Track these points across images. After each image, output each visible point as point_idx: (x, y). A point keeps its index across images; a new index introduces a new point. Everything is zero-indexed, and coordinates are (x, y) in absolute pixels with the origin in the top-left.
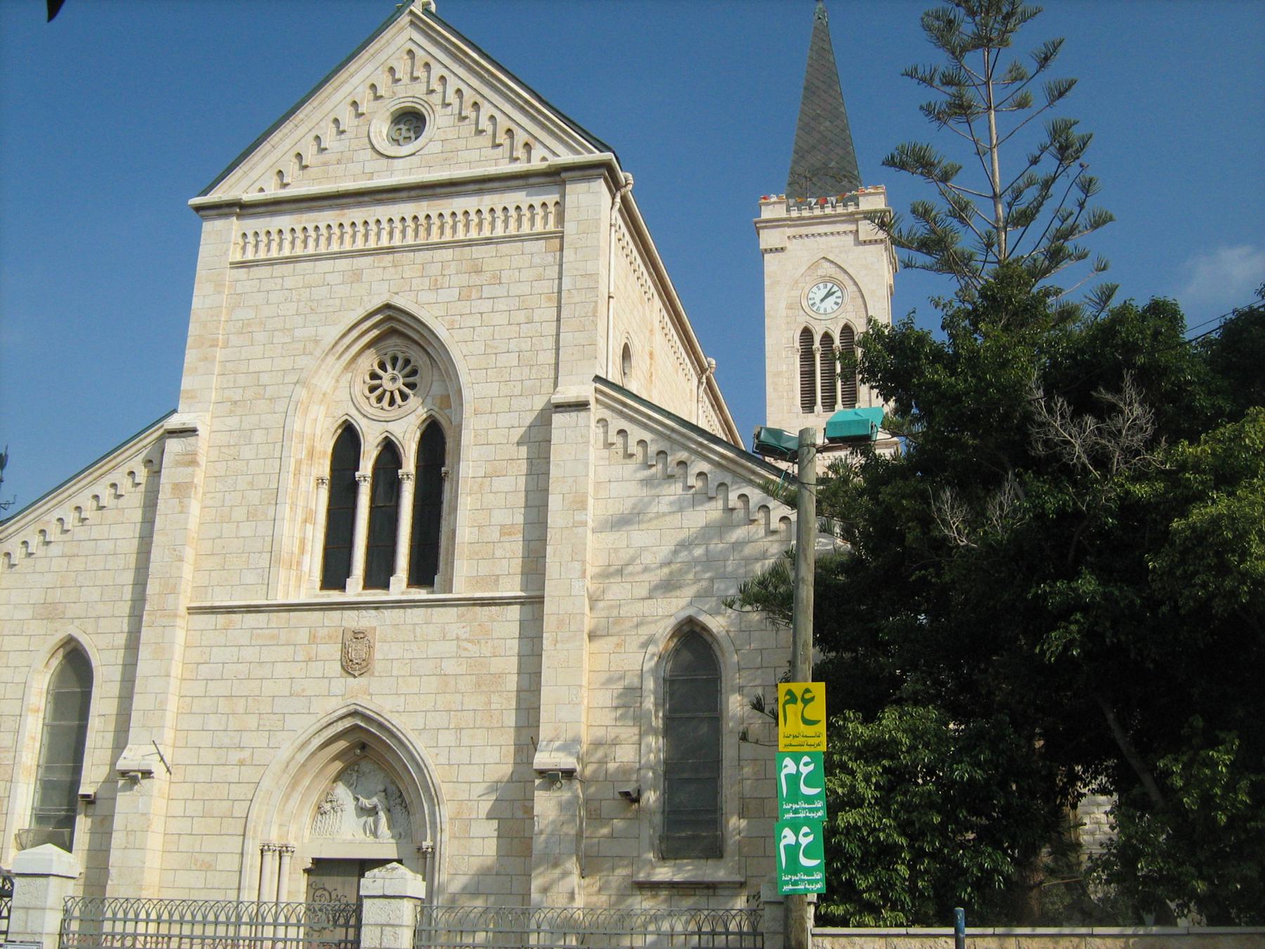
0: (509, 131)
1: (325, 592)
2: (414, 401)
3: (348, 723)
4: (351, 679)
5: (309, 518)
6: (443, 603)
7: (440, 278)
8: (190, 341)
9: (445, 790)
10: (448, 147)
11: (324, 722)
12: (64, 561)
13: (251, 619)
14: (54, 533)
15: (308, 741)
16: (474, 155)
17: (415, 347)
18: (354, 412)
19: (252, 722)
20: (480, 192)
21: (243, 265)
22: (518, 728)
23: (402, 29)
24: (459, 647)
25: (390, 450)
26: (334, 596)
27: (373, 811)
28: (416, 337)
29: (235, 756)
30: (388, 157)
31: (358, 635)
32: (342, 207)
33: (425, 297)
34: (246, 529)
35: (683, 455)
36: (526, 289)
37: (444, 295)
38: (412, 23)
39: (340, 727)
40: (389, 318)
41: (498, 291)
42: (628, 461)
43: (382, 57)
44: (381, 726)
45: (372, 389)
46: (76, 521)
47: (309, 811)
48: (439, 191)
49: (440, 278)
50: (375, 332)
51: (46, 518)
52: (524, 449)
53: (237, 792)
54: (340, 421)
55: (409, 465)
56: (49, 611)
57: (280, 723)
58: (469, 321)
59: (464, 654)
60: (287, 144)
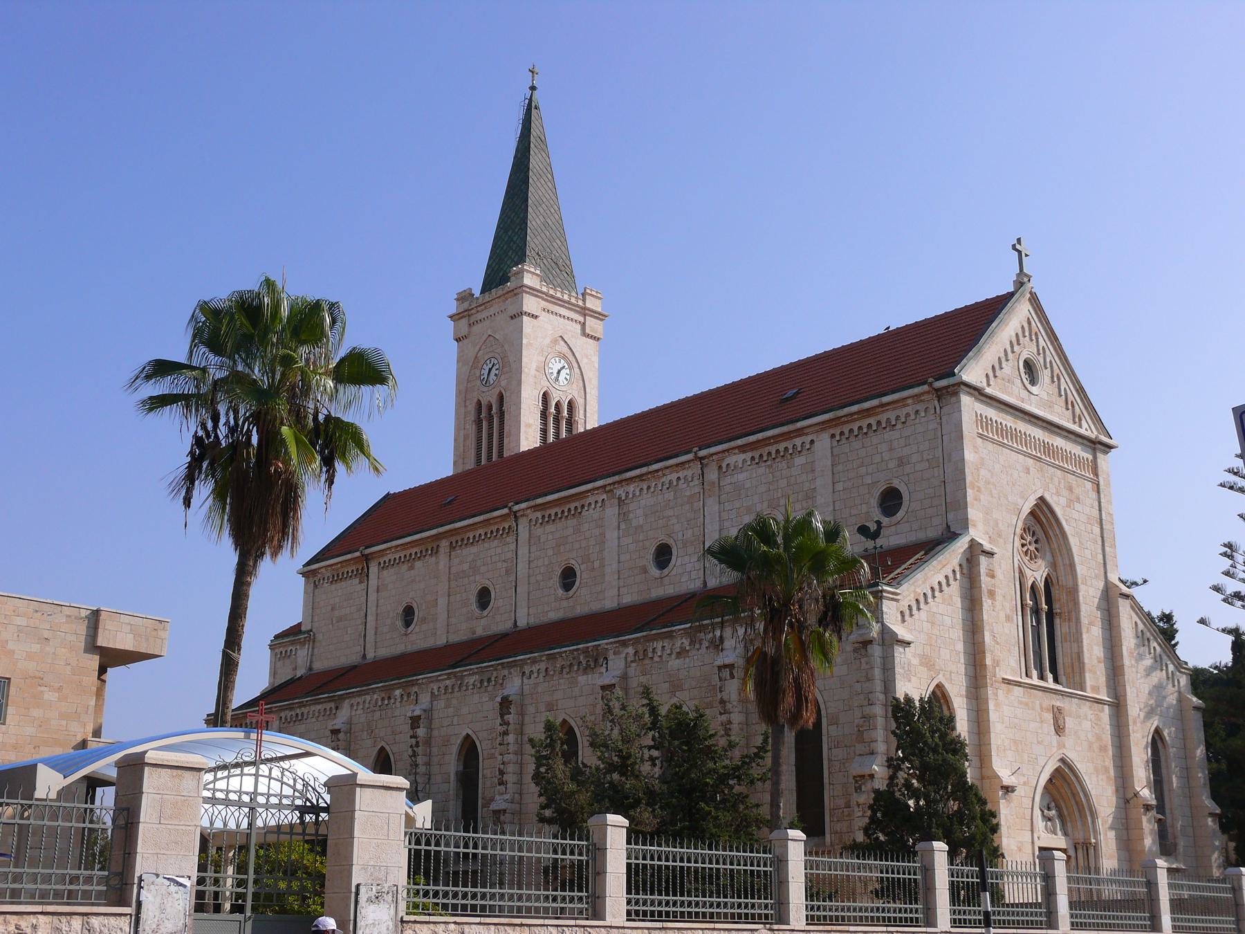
2: (1040, 561)
31: (1059, 709)
32: (1016, 417)
33: (1055, 498)
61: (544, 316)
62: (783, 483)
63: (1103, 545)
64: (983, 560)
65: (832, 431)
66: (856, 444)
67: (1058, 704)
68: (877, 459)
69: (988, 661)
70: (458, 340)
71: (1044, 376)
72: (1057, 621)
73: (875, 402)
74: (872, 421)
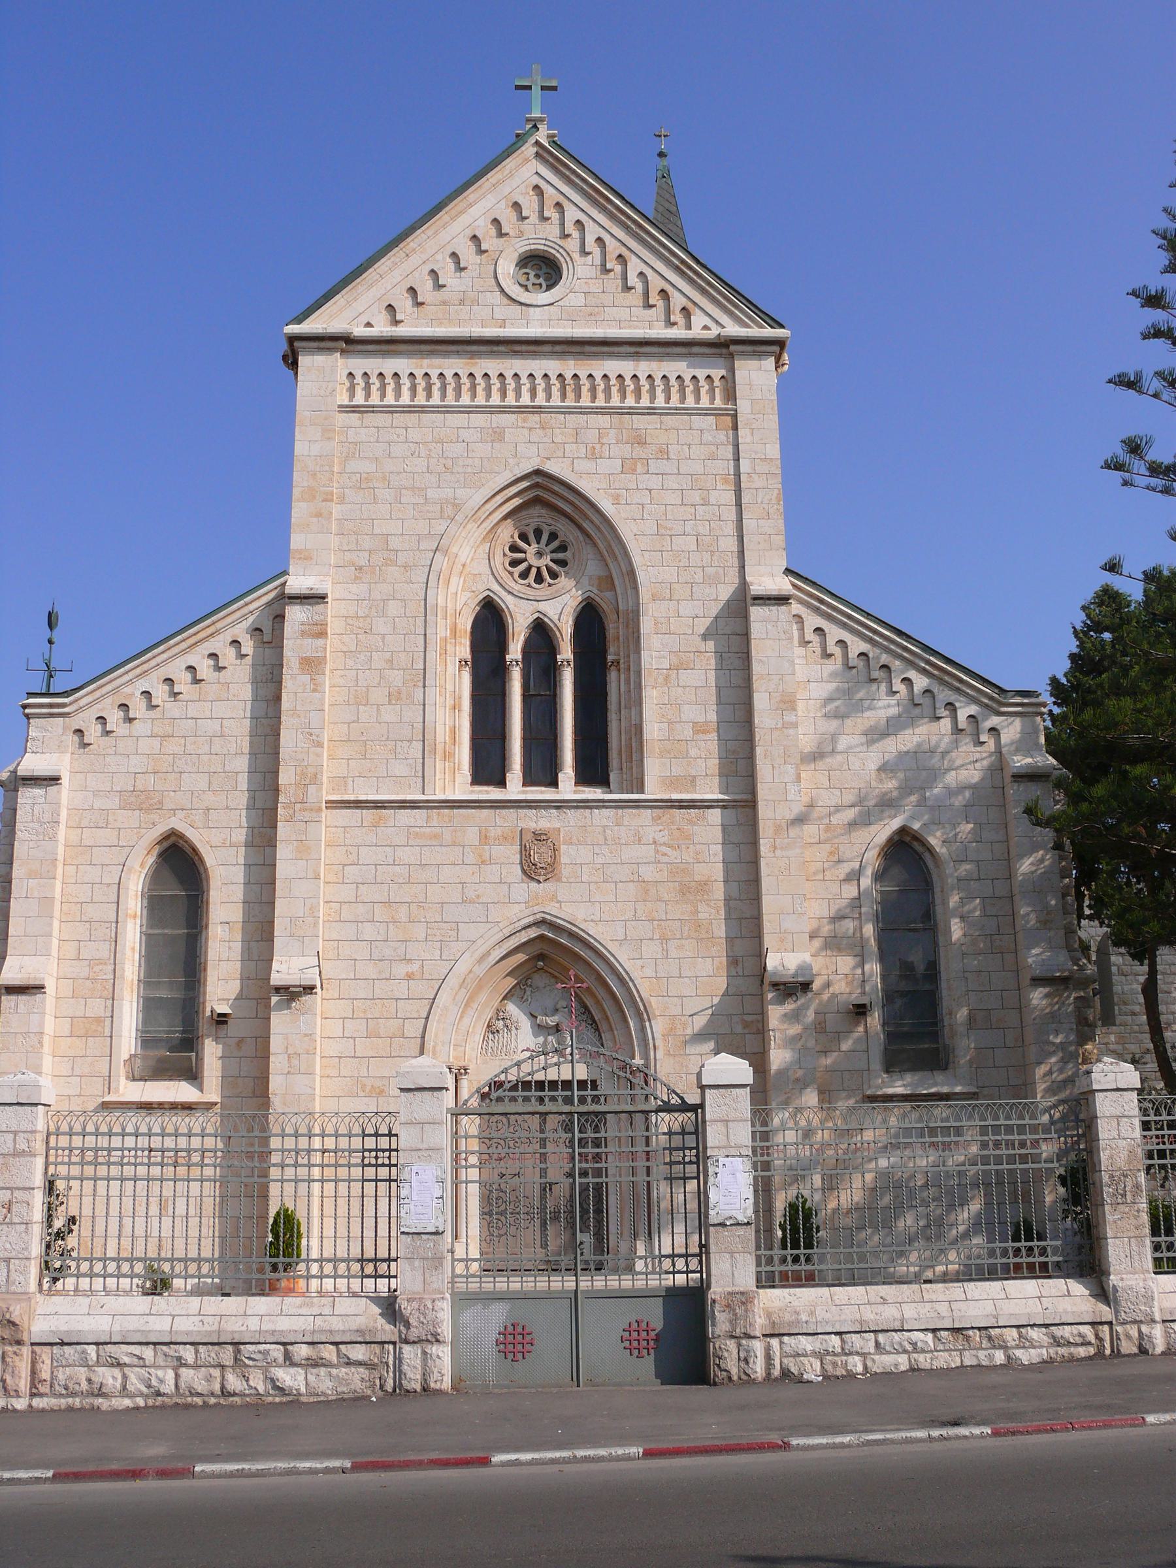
0: (663, 291)
1: (477, 788)
2: (564, 582)
3: (533, 933)
4: (533, 885)
5: (456, 707)
6: (636, 805)
7: (598, 447)
8: (296, 492)
9: (655, 1004)
10: (592, 300)
11: (507, 932)
12: (156, 742)
13: (405, 816)
14: (138, 707)
15: (488, 953)
16: (624, 313)
17: (564, 520)
18: (496, 587)
19: (419, 931)
20: (636, 356)
21: (354, 409)
22: (730, 940)
23: (527, 160)
24: (657, 852)
26: (492, 793)
27: (557, 1029)
28: (568, 509)
29: (401, 970)
30: (521, 304)
31: (540, 837)
32: (473, 355)
34: (389, 714)
36: (698, 467)
37: (604, 465)
38: (537, 154)
39: (524, 937)
40: (536, 486)
41: (664, 466)
42: (826, 661)
43: (506, 189)
44: (572, 935)
45: (514, 563)
46: (166, 697)
47: (481, 1029)
48: (588, 348)
49: (598, 447)
50: (517, 502)
51: (127, 690)
52: (711, 645)
53: (406, 1008)
54: (481, 597)
55: (566, 653)
56: (141, 801)
57: (454, 933)
58: (636, 497)
59: (665, 859)
60: (396, 276)
63: (740, 520)
67: (532, 825)
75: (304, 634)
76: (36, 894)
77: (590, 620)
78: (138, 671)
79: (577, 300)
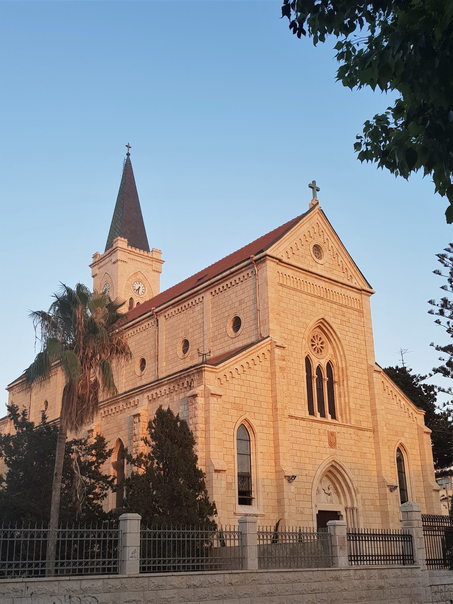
4: (331, 449)
21: (281, 285)
25: (319, 369)
33: (333, 320)
35: (396, 393)
56: (238, 407)
61: (129, 261)
62: (191, 321)
64: (277, 351)
65: (211, 291)
66: (221, 296)
68: (230, 303)
69: (279, 406)
70: (93, 277)
71: (326, 255)
72: (336, 386)
73: (228, 272)
74: (228, 282)
75: (279, 359)
76: (217, 437)
77: (329, 366)
78: (235, 361)
79: (327, 265)
